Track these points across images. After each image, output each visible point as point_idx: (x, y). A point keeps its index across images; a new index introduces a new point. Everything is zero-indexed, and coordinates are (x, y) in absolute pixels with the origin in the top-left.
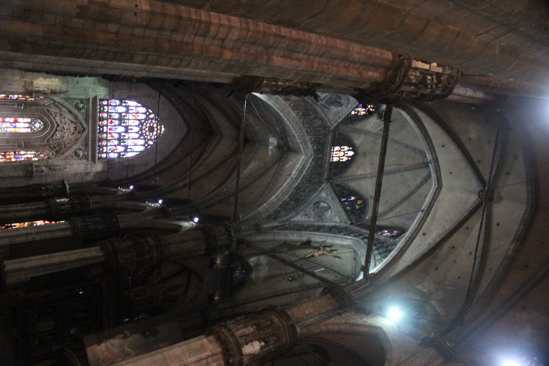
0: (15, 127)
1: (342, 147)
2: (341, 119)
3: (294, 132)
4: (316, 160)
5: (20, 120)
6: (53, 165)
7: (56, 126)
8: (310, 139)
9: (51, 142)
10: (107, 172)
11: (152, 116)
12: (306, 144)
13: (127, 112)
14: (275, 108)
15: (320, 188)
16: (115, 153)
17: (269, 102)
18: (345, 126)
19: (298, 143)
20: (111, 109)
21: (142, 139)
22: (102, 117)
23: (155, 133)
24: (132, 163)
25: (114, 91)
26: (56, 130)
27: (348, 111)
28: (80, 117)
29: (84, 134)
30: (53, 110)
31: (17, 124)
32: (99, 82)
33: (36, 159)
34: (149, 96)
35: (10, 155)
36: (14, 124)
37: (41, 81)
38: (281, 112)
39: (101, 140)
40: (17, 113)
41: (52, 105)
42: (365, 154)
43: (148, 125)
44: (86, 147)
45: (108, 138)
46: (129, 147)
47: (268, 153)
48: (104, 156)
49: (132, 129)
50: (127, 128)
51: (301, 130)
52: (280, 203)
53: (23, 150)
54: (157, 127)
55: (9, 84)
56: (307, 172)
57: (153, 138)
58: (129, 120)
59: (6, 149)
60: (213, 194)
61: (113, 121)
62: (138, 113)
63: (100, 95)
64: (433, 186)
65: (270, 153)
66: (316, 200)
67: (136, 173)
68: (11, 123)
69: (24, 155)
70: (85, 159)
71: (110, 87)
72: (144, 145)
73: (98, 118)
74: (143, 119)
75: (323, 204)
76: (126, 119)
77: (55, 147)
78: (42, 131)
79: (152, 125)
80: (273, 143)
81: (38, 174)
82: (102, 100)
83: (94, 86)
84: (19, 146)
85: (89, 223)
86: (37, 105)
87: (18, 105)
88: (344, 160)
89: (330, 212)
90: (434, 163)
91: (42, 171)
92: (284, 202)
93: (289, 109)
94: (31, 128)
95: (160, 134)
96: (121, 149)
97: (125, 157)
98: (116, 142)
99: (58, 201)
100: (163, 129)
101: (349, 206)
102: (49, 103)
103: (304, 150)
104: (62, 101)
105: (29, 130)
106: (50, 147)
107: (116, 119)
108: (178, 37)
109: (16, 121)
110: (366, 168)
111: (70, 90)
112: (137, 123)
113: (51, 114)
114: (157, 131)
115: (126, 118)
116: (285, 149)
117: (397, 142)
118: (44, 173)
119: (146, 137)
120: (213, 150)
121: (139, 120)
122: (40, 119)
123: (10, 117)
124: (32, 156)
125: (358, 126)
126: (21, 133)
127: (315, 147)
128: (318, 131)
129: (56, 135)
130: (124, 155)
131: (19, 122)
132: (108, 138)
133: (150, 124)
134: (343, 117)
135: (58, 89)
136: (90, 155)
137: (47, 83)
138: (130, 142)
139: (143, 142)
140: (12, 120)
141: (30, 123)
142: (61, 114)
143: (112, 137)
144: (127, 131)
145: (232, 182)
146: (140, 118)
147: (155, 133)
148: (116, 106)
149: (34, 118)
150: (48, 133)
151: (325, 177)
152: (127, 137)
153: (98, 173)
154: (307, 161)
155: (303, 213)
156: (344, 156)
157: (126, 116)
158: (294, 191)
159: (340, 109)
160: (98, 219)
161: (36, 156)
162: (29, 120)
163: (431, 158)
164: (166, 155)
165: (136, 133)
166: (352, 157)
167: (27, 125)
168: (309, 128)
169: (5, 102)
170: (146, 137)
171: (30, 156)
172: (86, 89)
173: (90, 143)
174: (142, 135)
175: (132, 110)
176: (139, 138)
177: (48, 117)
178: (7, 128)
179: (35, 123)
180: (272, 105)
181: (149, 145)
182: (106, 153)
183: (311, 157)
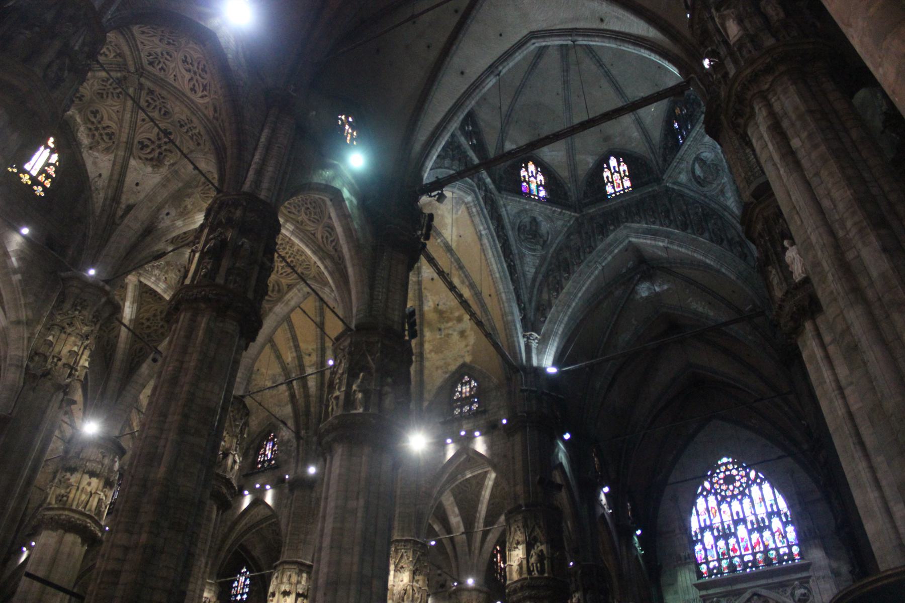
3: (596, 272)
8: (602, 240)
11: (707, 485)
12: (610, 245)
13: (711, 528)
15: (675, 187)
16: (786, 532)
18: (569, 193)
19: (613, 257)
21: (750, 491)
22: (728, 567)
23: (734, 472)
25: (679, 558)
27: (536, 205)
29: (764, 592)
32: (673, 584)
38: (569, 306)
39: (768, 561)
42: (607, 139)
43: (724, 487)
44: (787, 586)
45: (762, 549)
46: (769, 510)
47: (667, 290)
48: (795, 550)
49: (738, 513)
50: (736, 523)
51: (590, 262)
52: (716, 247)
56: (654, 223)
58: (722, 522)
64: (537, 45)
65: (665, 287)
66: (695, 186)
70: (808, 582)
71: (675, 567)
72: (760, 485)
74: (716, 499)
75: (698, 172)
76: (723, 526)
82: (700, 574)
83: (680, 592)
89: (704, 154)
90: (497, 68)
92: (711, 240)
93: (561, 296)
95: (733, 463)
96: (776, 523)
97: (788, 513)
98: (767, 534)
100: (725, 460)
103: (621, 243)
107: (727, 544)
121: (719, 504)
125: (563, 173)
127: (612, 228)
128: (586, 233)
130: (785, 514)
132: (762, 549)
133: (721, 485)
136: (799, 576)
138: (761, 512)
139: (755, 489)
146: (715, 502)
155: (722, 199)
156: (619, 172)
157: (718, 529)
158: (689, 231)
159: (540, 218)
163: (492, 77)
165: (741, 503)
168: (584, 252)
173: (776, 580)
174: (743, 493)
181: (757, 477)
182: (790, 547)
183: (629, 227)
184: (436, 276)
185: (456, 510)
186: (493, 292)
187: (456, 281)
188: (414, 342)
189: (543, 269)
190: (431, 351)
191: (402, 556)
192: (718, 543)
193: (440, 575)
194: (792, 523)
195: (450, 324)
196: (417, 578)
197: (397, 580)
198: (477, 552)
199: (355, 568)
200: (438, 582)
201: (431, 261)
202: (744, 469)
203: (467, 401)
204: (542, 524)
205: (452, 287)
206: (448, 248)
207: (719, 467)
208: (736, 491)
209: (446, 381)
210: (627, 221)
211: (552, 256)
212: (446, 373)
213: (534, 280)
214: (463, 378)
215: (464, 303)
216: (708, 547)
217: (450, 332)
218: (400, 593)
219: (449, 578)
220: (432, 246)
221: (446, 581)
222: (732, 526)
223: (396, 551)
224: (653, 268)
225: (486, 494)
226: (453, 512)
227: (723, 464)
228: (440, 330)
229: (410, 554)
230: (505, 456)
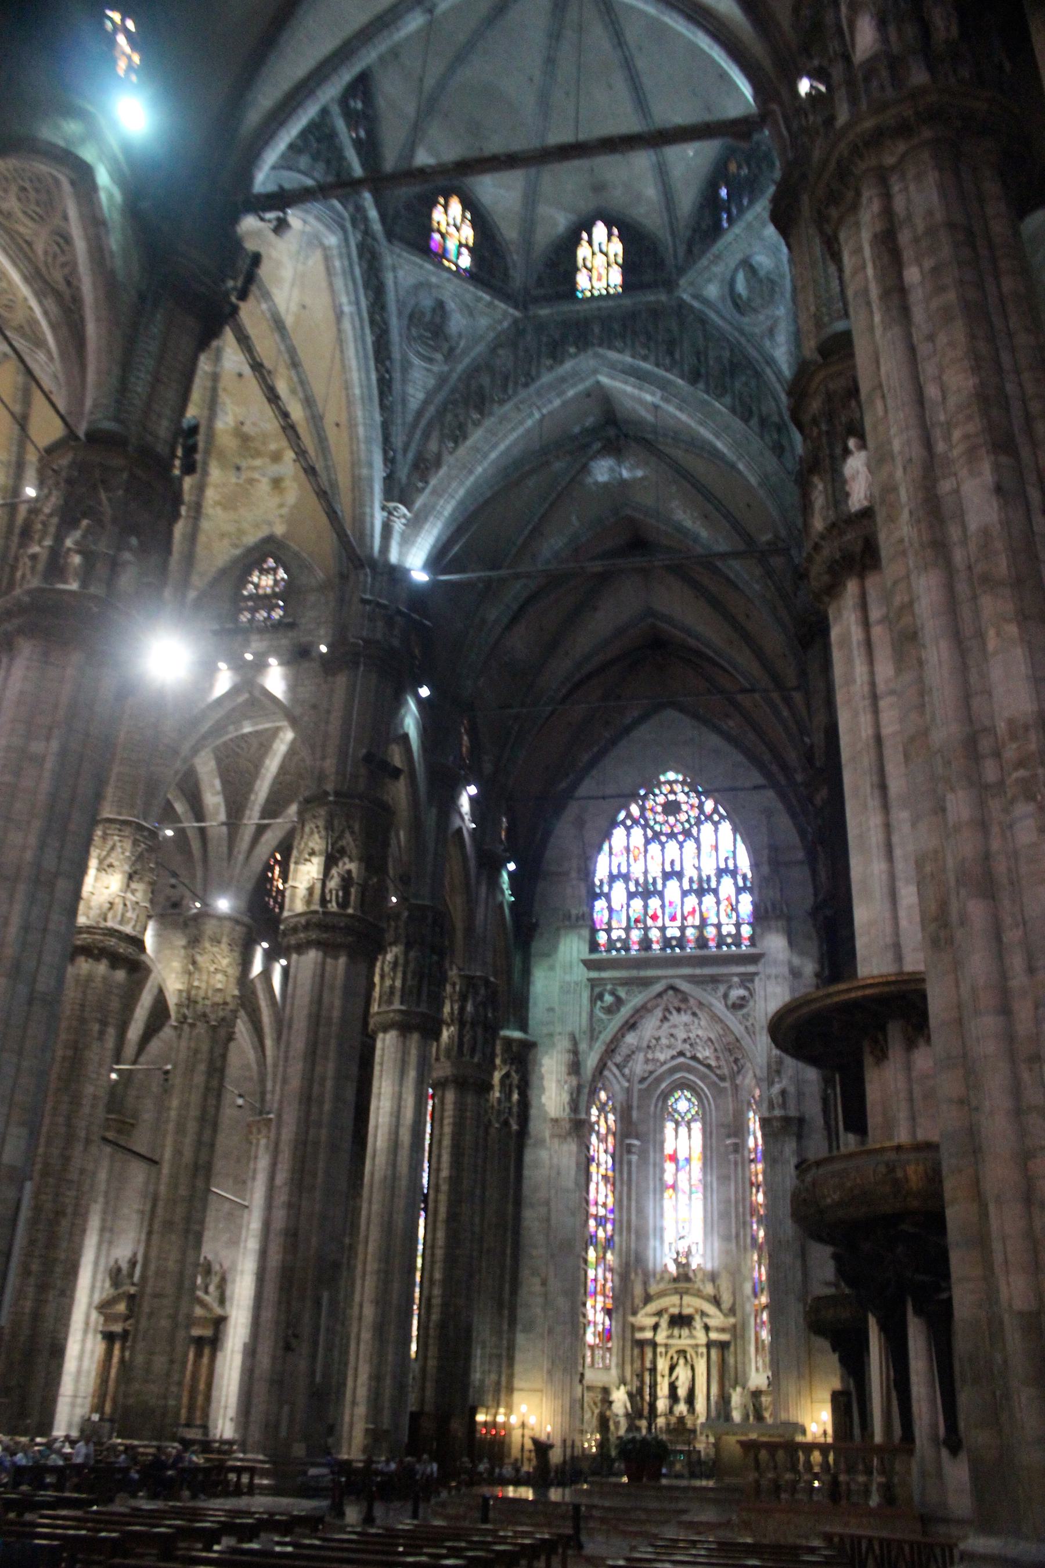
0: (688, 1160)
2: (480, 294)
4: (608, 340)
5: (668, 1150)
6: (769, 1066)
7: (681, 1060)
8: (551, 368)
9: (726, 1071)
10: (789, 919)
11: (635, 810)
12: (563, 380)
13: (626, 878)
14: (461, 492)
16: (737, 902)
17: (446, 513)
18: (511, 272)
19: (565, 404)
20: (619, 921)
21: (699, 831)
22: (640, 943)
23: (681, 798)
24: (766, 852)
25: (570, 917)
26: (694, 1058)
27: (449, 280)
28: (637, 999)
29: (684, 986)
30: (638, 1066)
31: (681, 1156)
34: (580, 823)
35: (757, 1175)
36: (682, 1163)
37: (550, 1098)
38: (471, 472)
39: (702, 942)
40: (652, 1154)
41: (627, 1071)
42: (599, 188)
43: (660, 818)
45: (697, 923)
46: (722, 866)
47: (643, 479)
48: (746, 931)
49: (672, 863)
50: (667, 876)
51: (522, 402)
52: (738, 424)
53: (744, 1141)
55: (559, 1173)
56: (645, 358)
58: (646, 873)
59: (743, 1183)
61: (651, 912)
62: (628, 849)
63: (579, 951)
65: (639, 473)
66: (728, 310)
67: (794, 838)
70: (752, 981)
71: (558, 929)
72: (716, 824)
73: (643, 954)
74: (645, 835)
75: (741, 286)
79: (659, 809)
80: (611, 470)
81: (792, 1103)
82: (594, 946)
83: (558, 969)
86: (630, 1108)
87: (629, 1152)
91: (783, 1093)
92: (733, 410)
93: (462, 451)
95: (683, 783)
98: (709, 900)
100: (671, 776)
103: (582, 380)
104: (599, 1047)
105: (697, 1126)
106: (739, 1072)
107: (646, 907)
109: (673, 1158)
110: (635, 177)
111: (569, 1029)
112: (654, 848)
113: (651, 1073)
115: (641, 881)
116: (612, 432)
117: (544, 101)
118: (792, 1089)
119: (693, 821)
121: (647, 842)
123: (663, 1171)
125: (509, 232)
126: (704, 1147)
128: (527, 350)
130: (744, 877)
131: (675, 1151)
134: (472, 288)
135: (566, 1058)
136: (741, 969)
137: (554, 1085)
140: (669, 1166)
141: (677, 1123)
144: (679, 875)
145: (736, 568)
148: (610, 909)
149: (664, 1113)
150: (703, 1077)
151: (663, 298)
153: (791, 943)
154: (612, 365)
155: (768, 343)
158: (701, 385)
159: (451, 305)
162: (670, 1126)
164: (745, 761)
165: (681, 847)
166: (609, 226)
167: (683, 1130)
168: (516, 383)
169: (622, 1184)
170: (693, 821)
172: (565, 989)
173: (707, 971)
174: (687, 833)
175: (619, 866)
176: (697, 841)
177: (659, 1080)
179: (676, 1111)
180: (453, 503)
181: (715, 810)
182: (738, 925)
184: (247, 370)
185: (217, 783)
186: (343, 419)
187: (282, 387)
188: (188, 482)
189: (439, 398)
190: (218, 503)
191: (113, 848)
192: (632, 902)
193: (173, 886)
194: (751, 890)
195: (258, 462)
196: (134, 886)
197: (98, 885)
198: (241, 858)
199: (29, 856)
200: (168, 898)
201: (244, 341)
202: (699, 795)
203: (264, 601)
204: (357, 827)
205: (273, 397)
206: (278, 325)
207: (659, 785)
208: (678, 828)
209: (235, 561)
210: (600, 345)
211: (460, 379)
212: (236, 546)
213: (420, 413)
214: (265, 561)
215: (289, 428)
216: (616, 906)
217: (256, 476)
218: (100, 908)
219: (188, 894)
220: (250, 313)
221: (182, 898)
222: (659, 882)
223: (105, 837)
224: (626, 436)
225: (272, 765)
226: (213, 786)
228: (238, 468)
229: (128, 845)
230: (314, 707)
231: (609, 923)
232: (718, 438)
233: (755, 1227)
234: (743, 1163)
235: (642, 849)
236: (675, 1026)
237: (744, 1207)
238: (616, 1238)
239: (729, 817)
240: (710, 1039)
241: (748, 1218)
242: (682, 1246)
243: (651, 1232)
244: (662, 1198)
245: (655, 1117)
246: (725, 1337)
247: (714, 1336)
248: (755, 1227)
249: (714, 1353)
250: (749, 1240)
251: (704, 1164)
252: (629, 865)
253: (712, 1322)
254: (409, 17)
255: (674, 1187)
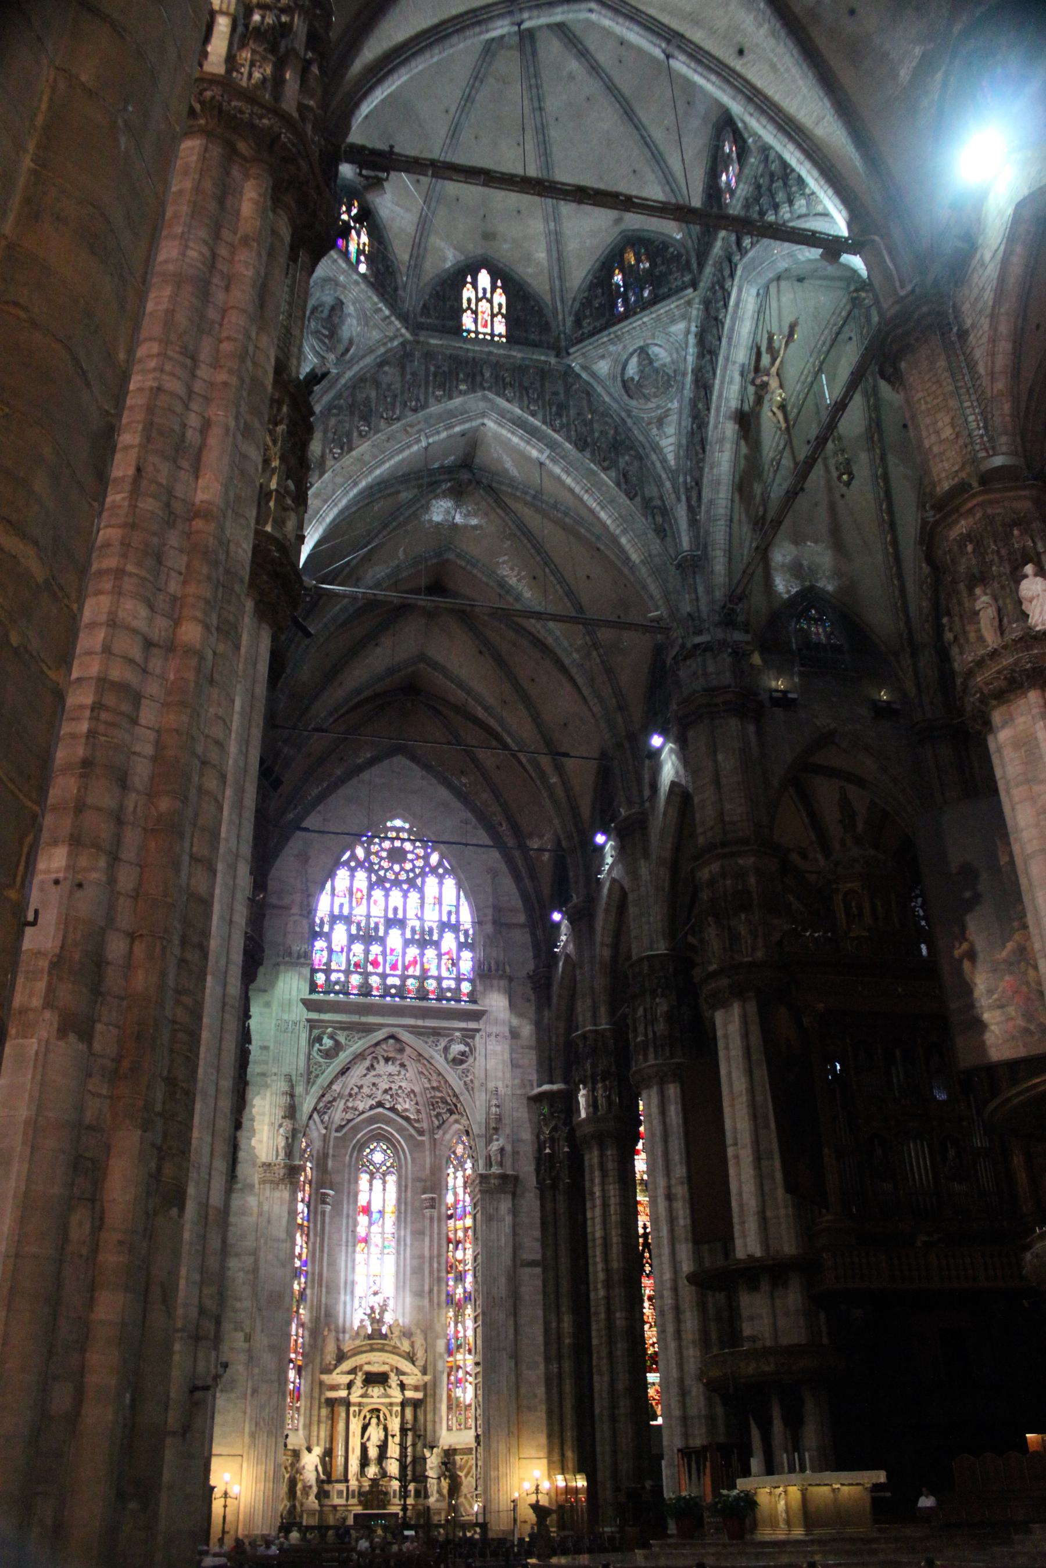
0: (381, 1213)
1: (465, 305)
2: (381, 305)
3: (415, 448)
4: (500, 386)
5: (362, 1200)
6: (487, 1124)
7: (380, 1110)
8: (439, 400)
9: (425, 1125)
10: (511, 979)
11: (360, 852)
12: (452, 414)
13: (348, 920)
14: (344, 502)
15: (584, 375)
16: (459, 958)
17: (328, 520)
18: (400, 292)
19: (449, 437)
21: (423, 882)
22: (360, 987)
23: (408, 846)
24: (489, 912)
25: (290, 954)
26: (392, 1109)
27: (357, 283)
28: (358, 1045)
29: (405, 1036)
30: (338, 1115)
31: (375, 1207)
32: (265, 991)
33: (469, 1165)
34: (304, 858)
35: (456, 1231)
36: (376, 1216)
37: (261, 1142)
38: (356, 484)
39: (422, 994)
41: (326, 1117)
42: (489, 236)
43: (385, 864)
44: (439, 1034)
45: (417, 973)
46: (445, 919)
47: (475, 527)
48: (466, 987)
49: (396, 909)
50: (390, 923)
51: (411, 426)
52: (623, 499)
53: (441, 1197)
54: (392, 839)
55: (269, 1222)
56: (533, 414)
57: (421, 852)
58: (368, 916)
59: (439, 1239)
60: (586, 692)
61: (371, 958)
62: (350, 891)
63: (298, 990)
65: (474, 522)
66: (617, 390)
67: (517, 902)
68: (371, 1224)
69: (455, 1194)
70: (473, 1037)
71: (278, 964)
72: (441, 877)
73: (362, 999)
74: (369, 878)
75: (632, 370)
76: (368, 923)
77: (438, 1115)
78: (394, 1146)
79: (384, 854)
80: (448, 512)
81: (508, 1162)
82: (313, 987)
83: (275, 1006)
84: (433, 1207)
85: (650, 1035)
86: (325, 1156)
87: (324, 1202)
88: (503, 300)
89: (656, 349)
91: (502, 1150)
92: (618, 485)
93: (348, 460)
94: (384, 1175)
95: (409, 831)
96: (449, 942)
97: (471, 932)
98: (430, 953)
99: (583, 1115)
100: (398, 823)
101: (642, 289)
102: (320, 1126)
103: (470, 419)
104: (315, 1090)
105: (392, 1179)
106: (439, 1127)
107: (367, 952)
108: (141, 771)
109: (367, 1210)
111: (286, 1070)
112: (378, 894)
113: (349, 1121)
114: (403, 840)
116: (465, 476)
118: (509, 1148)
119: (417, 871)
120: (461, 685)
121: (371, 887)
122: (361, 1150)
123: (356, 1224)
124: (460, 1174)
125: (401, 253)
126: (399, 1200)
127: (463, 387)
128: (414, 374)
129: (406, 1110)
130: (466, 932)
131: (369, 1203)
132: (417, 973)
133: (382, 858)
134: (375, 299)
135: (284, 1100)
136: (463, 1025)
137: (266, 1128)
138: (432, 917)
139: (431, 881)
140: (363, 1219)
142: (350, 1095)
143: (415, 962)
144: (401, 923)
145: (554, 633)
147: (408, 846)
148: (331, 951)
149: (358, 1164)
150: (401, 1130)
151: (553, 360)
152: (417, 924)
153: (512, 1005)
154: (502, 413)
155: (655, 431)
156: (490, 301)
157: (359, 924)
159: (350, 309)
160: (640, 1012)
161: (461, 1165)
162: (364, 1177)
166: (494, 276)
167: (377, 1183)
169: (315, 1235)
171: (460, 1182)
172: (282, 1028)
173: (430, 1023)
174: (412, 883)
175: (341, 905)
176: (421, 891)
177: (356, 1129)
178: (383, 1233)
179: (371, 1162)
180: (336, 511)
181: (440, 864)
182: (459, 980)
183: (490, 401)
192: (353, 947)
208: (403, 876)
210: (489, 389)
216: (336, 948)
224: (478, 483)
227: (394, 829)
231: (328, 963)
232: (602, 508)
233: (451, 1283)
234: (439, 1220)
235: (365, 892)
236: (379, 1076)
237: (439, 1263)
238: (308, 1292)
239: (451, 872)
240: (413, 1091)
241: (443, 1274)
242: (376, 1301)
243: (342, 1285)
244: (354, 1251)
245: (350, 1165)
246: (419, 1395)
247: (409, 1394)
248: (451, 1283)
249: (409, 1412)
250: (443, 1297)
251: (398, 1218)
252: (351, 908)
253: (407, 1380)
254: (499, 23)
255: (365, 1240)
